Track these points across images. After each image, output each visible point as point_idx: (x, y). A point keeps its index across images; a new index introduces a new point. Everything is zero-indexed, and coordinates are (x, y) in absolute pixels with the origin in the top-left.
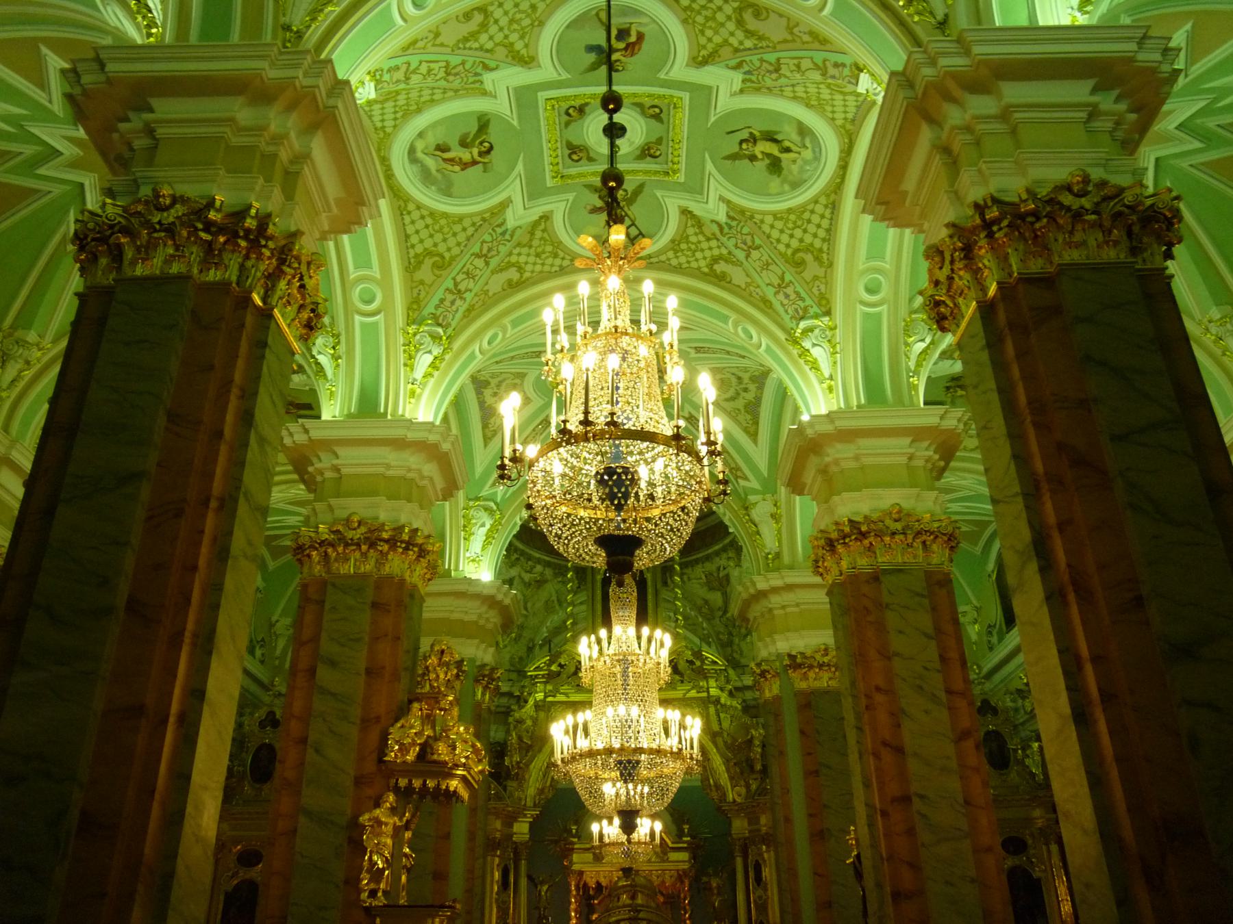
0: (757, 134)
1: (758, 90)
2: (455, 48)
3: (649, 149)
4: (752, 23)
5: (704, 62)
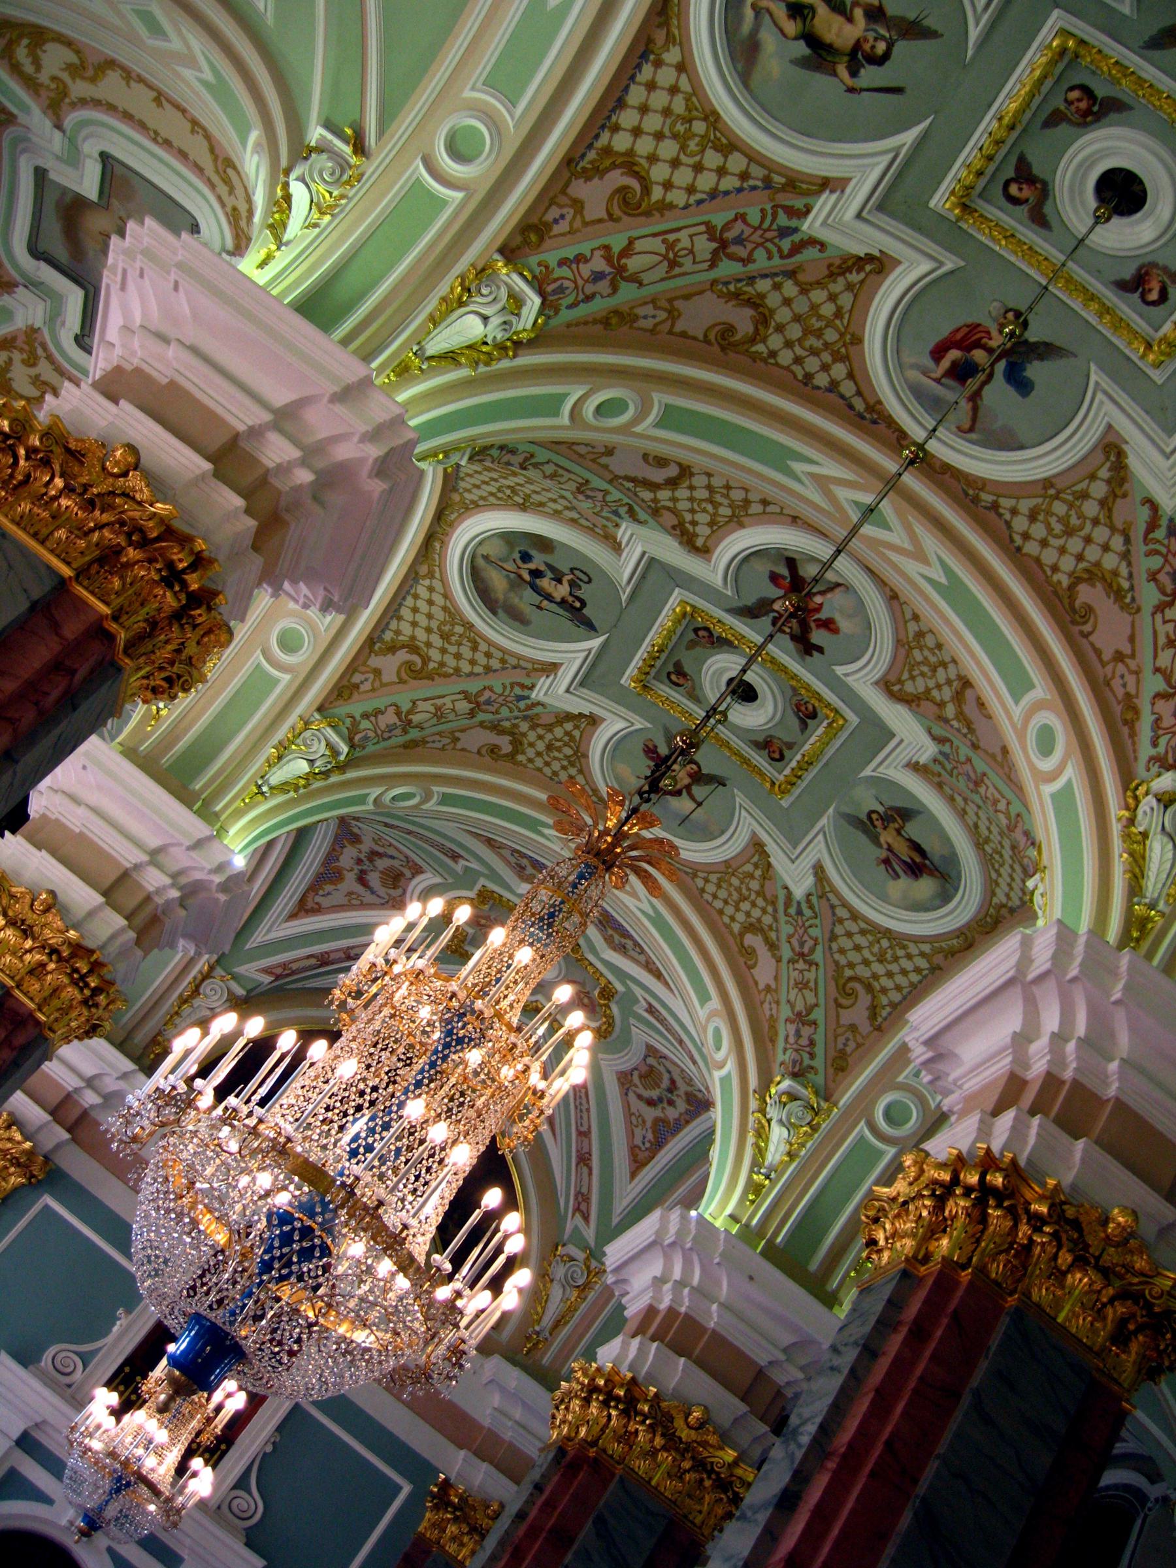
0: (842, 70)
1: (793, 182)
2: (1133, 609)
3: (1087, 113)
4: (743, 320)
5: (860, 262)
